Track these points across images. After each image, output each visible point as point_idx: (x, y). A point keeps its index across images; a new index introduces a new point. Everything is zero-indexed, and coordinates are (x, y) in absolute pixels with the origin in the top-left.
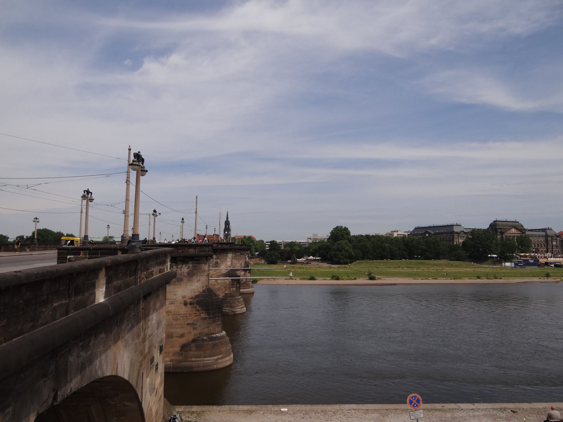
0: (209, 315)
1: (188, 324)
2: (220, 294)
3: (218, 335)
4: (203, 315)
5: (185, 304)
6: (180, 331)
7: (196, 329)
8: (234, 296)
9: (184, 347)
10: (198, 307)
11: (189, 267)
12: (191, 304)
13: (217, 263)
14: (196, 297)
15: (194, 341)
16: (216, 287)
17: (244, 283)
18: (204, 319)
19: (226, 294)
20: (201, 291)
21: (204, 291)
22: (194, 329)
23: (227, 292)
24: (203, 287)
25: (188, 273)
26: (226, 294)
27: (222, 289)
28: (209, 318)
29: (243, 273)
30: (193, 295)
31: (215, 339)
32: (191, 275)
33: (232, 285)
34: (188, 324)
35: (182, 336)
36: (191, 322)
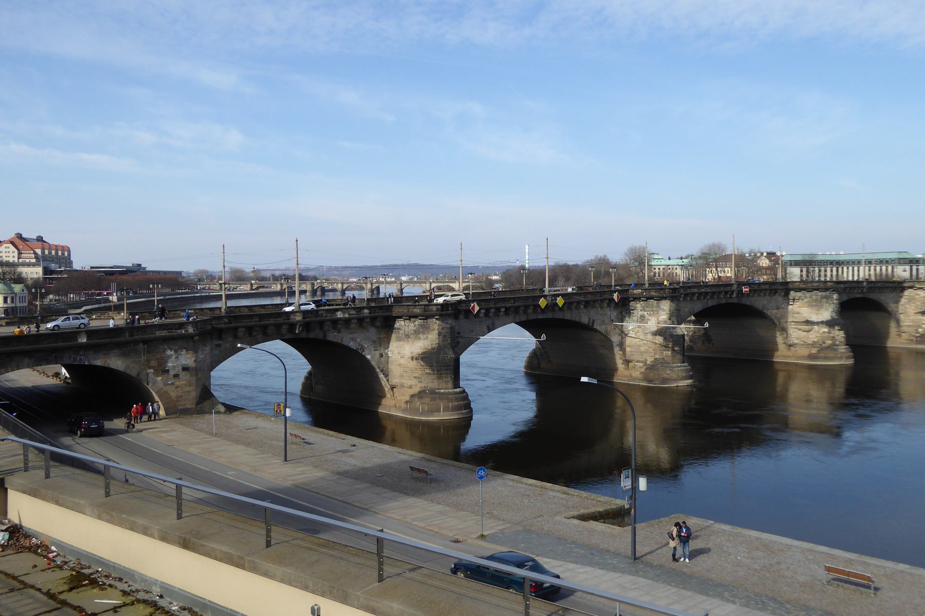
4: (428, 371)
5: (412, 359)
6: (409, 383)
9: (412, 396)
12: (417, 359)
13: (643, 317)
14: (423, 353)
16: (643, 349)
19: (656, 359)
21: (433, 349)
23: (657, 356)
26: (656, 359)
30: (420, 351)
31: (436, 393)
32: (417, 333)
35: (410, 387)
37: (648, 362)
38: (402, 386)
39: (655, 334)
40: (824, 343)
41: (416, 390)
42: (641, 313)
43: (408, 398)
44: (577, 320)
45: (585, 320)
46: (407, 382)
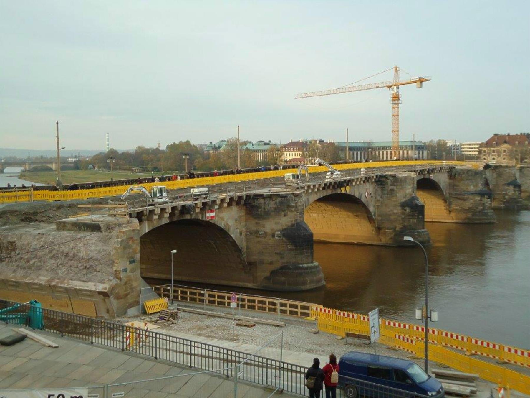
0: (296, 246)
1: (277, 254)
2: (397, 225)
3: (305, 265)
4: (290, 247)
7: (283, 258)
8: (415, 229)
9: (273, 273)
10: (284, 239)
11: (276, 203)
13: (392, 190)
15: (282, 268)
16: (392, 217)
17: (480, 212)
18: (291, 250)
20: (290, 224)
21: (293, 225)
22: (282, 258)
24: (291, 221)
25: (275, 209)
27: (399, 221)
28: (296, 249)
29: (478, 198)
33: (413, 216)
34: (277, 254)
35: (271, 263)
36: (278, 252)
37: (397, 229)
38: (262, 262)
39: (403, 205)
40: (477, 208)
41: (277, 266)
42: (390, 187)
43: (267, 274)
44: (353, 195)
45: (357, 195)
46: (267, 258)
